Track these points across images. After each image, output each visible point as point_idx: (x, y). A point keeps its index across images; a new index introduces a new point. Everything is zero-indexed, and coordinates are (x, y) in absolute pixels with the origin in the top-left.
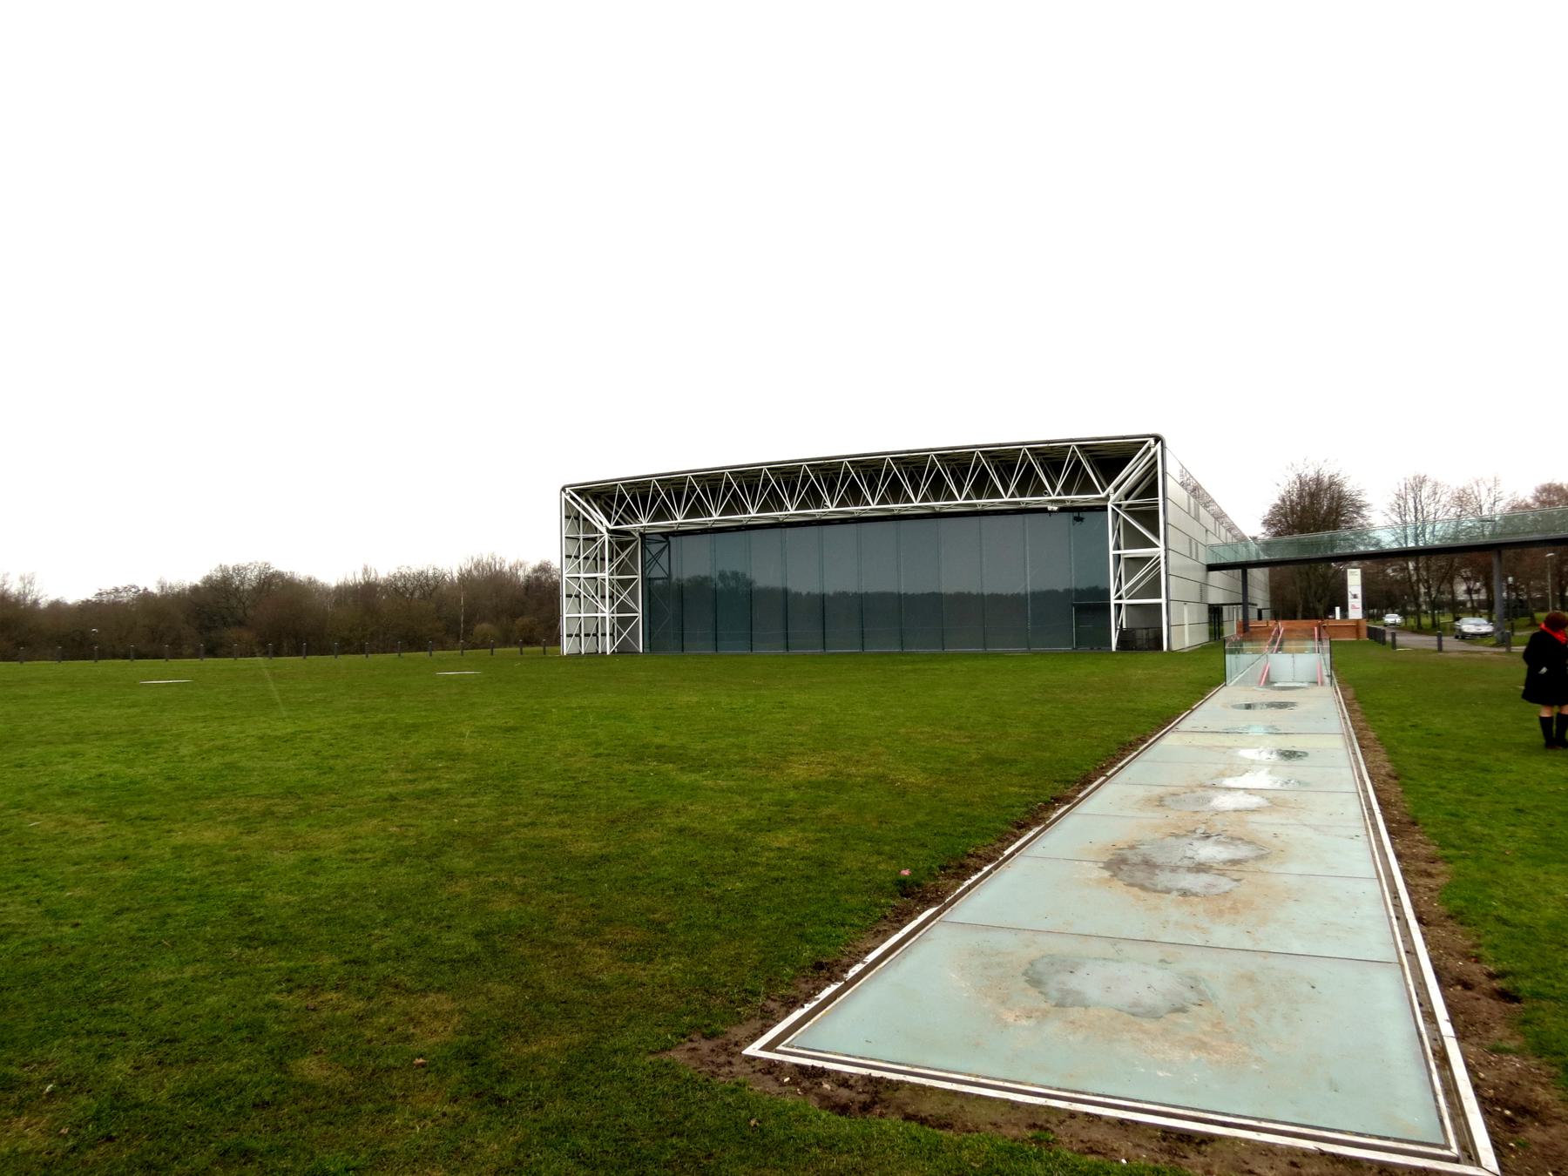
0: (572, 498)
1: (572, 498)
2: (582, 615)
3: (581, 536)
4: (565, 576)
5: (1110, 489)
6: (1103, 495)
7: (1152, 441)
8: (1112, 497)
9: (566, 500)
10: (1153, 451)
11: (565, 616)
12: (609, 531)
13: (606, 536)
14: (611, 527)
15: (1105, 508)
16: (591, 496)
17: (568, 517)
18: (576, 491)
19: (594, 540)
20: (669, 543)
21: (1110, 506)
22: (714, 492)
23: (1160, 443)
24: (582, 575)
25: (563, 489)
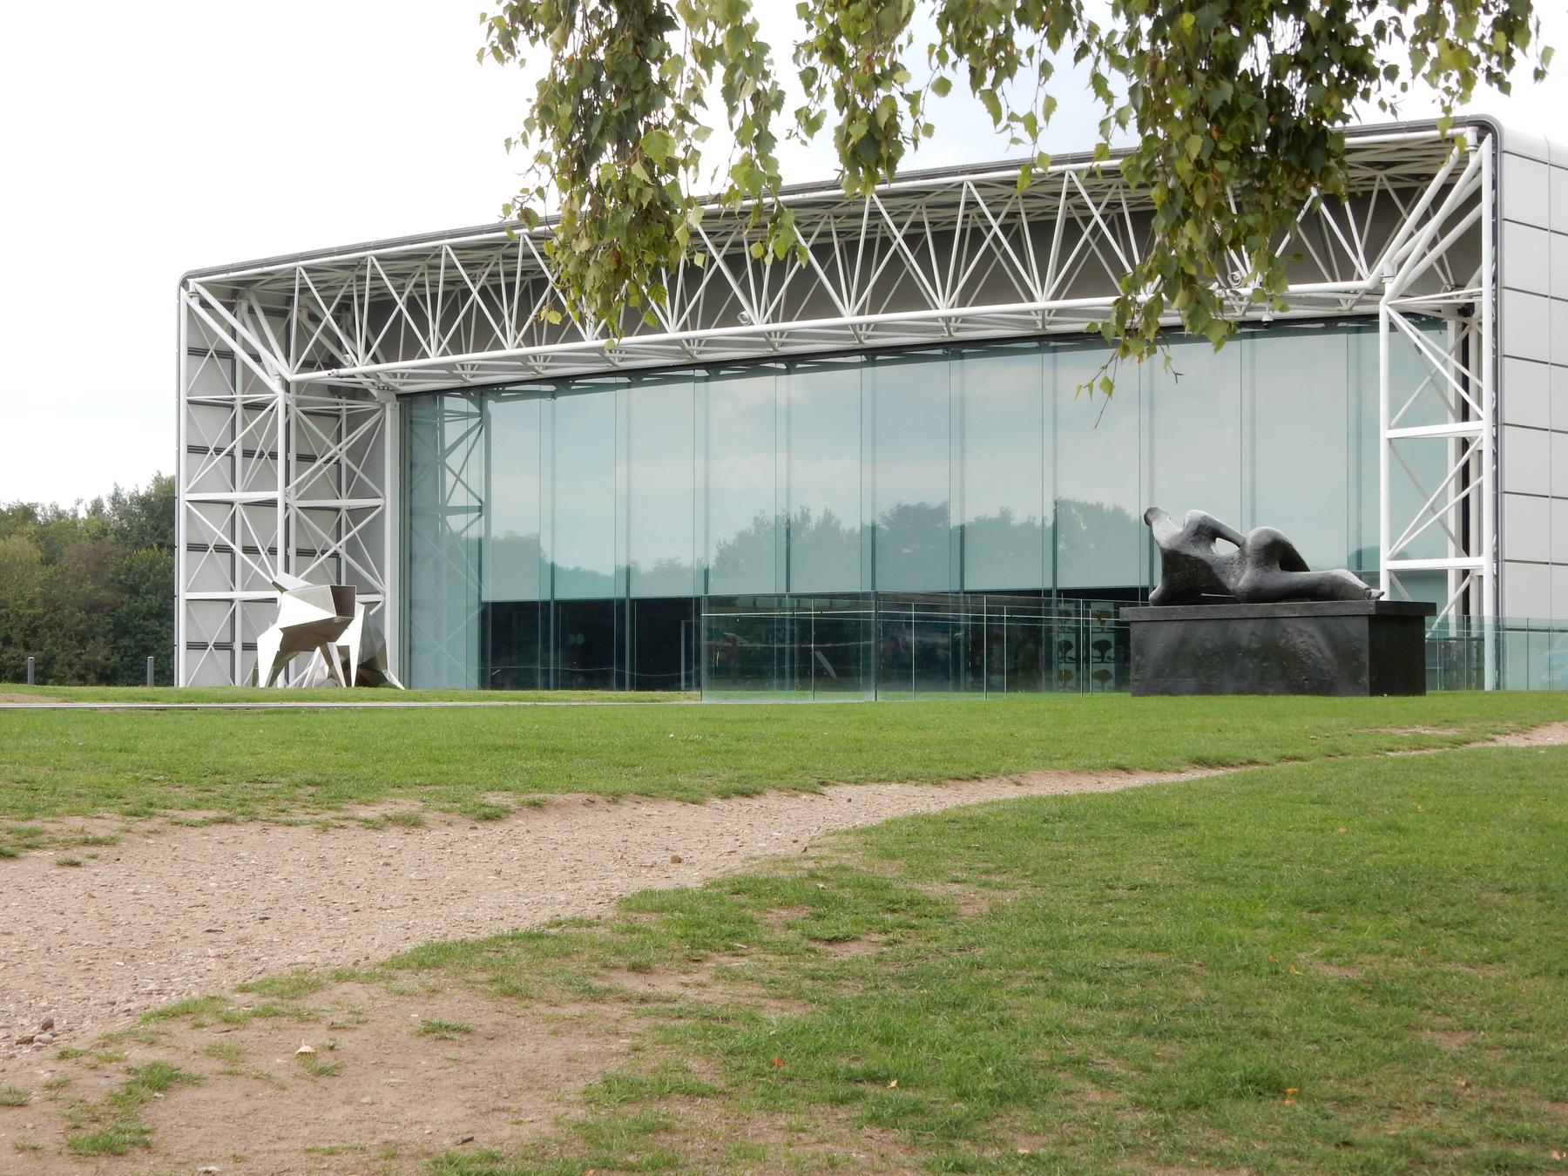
0: (204, 304)
1: (204, 304)
2: (239, 594)
3: (239, 396)
4: (184, 497)
5: (1384, 264)
6: (1367, 283)
7: (1470, 134)
8: (1389, 288)
9: (190, 309)
10: (1473, 159)
11: (183, 595)
12: (287, 386)
13: (280, 397)
14: (292, 377)
15: (1368, 322)
16: (260, 301)
17: (192, 352)
18: (208, 286)
19: (260, 406)
20: (484, 420)
21: (1384, 310)
22: (1042, 230)
23: (1489, 137)
24: (239, 496)
25: (184, 284)
